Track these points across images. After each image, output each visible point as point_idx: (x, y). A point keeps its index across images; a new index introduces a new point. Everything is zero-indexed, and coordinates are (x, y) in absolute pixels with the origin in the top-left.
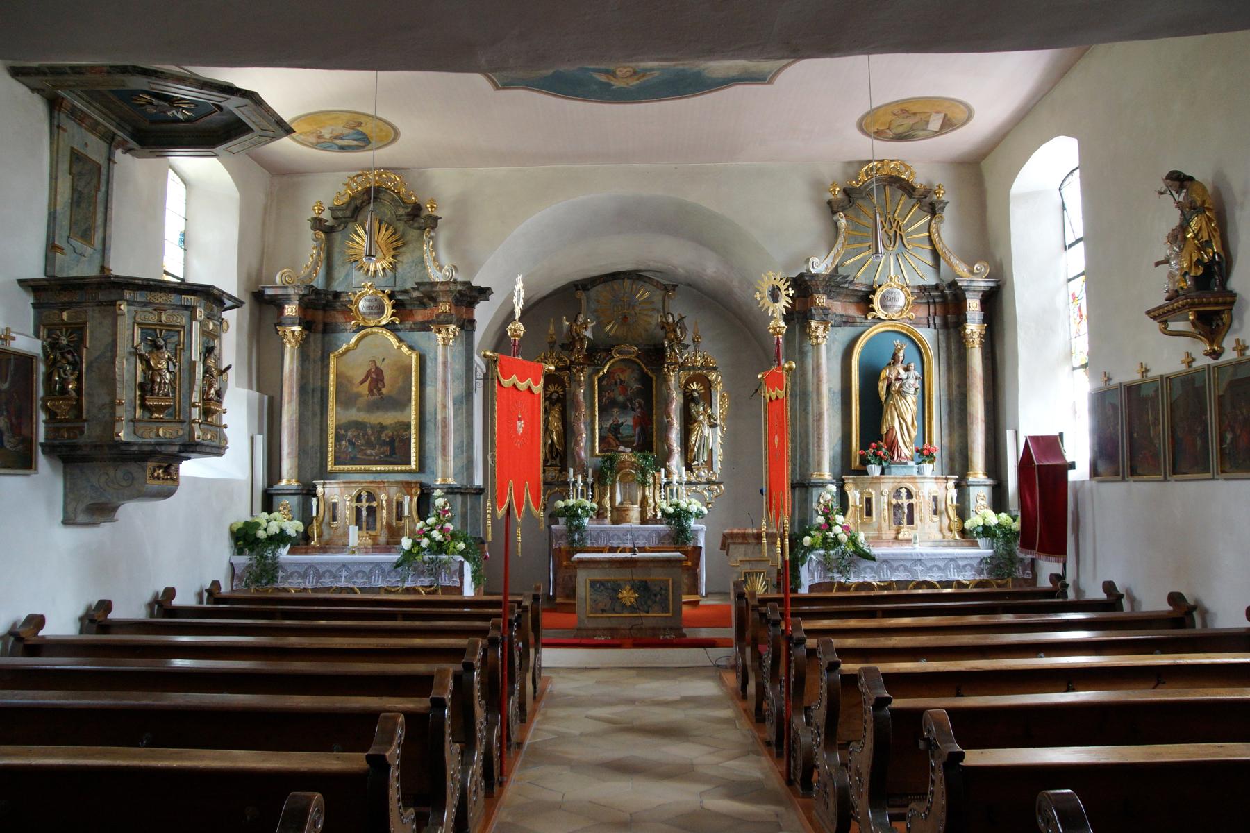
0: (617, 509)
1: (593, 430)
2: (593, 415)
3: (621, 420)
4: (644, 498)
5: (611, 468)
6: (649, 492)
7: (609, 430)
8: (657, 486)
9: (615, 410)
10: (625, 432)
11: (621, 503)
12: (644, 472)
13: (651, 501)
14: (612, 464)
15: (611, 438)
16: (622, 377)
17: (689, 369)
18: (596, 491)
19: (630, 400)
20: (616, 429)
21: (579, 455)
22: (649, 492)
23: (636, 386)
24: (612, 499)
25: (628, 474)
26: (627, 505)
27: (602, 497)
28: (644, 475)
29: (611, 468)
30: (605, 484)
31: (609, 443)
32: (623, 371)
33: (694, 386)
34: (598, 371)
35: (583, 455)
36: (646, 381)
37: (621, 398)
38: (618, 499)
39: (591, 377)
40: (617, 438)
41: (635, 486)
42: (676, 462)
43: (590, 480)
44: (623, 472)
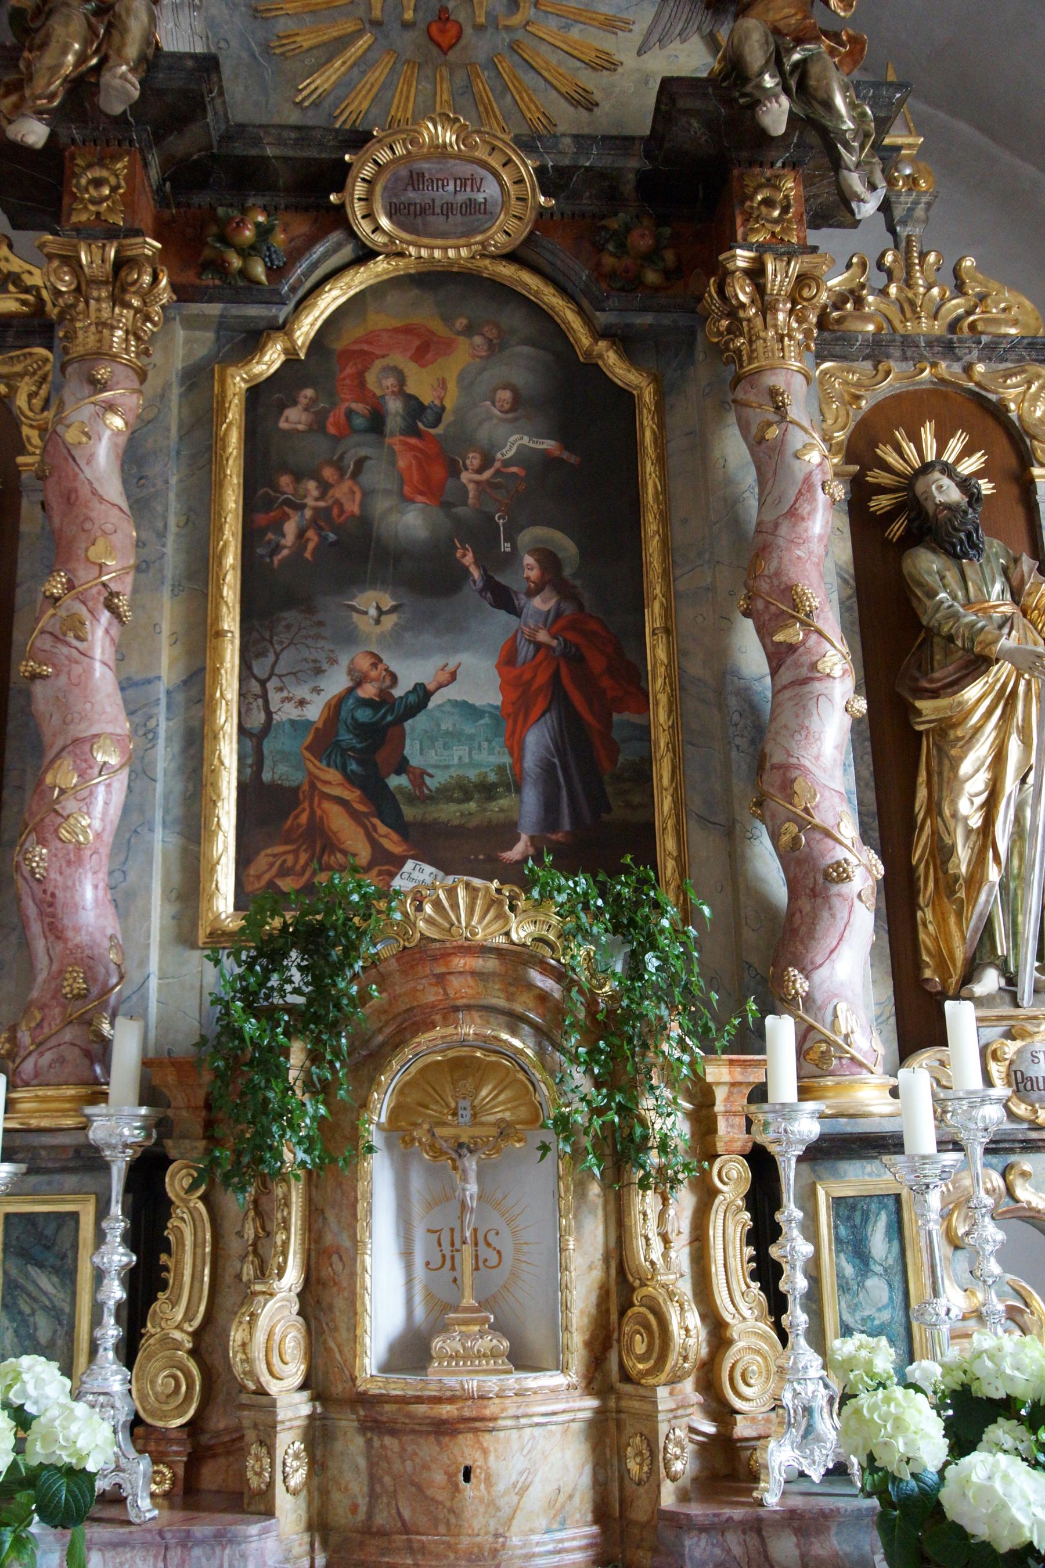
0: (375, 1414)
1: (196, 743)
2: (200, 637)
3: (411, 673)
4: (623, 1286)
5: (318, 1017)
6: (662, 1230)
7: (324, 741)
8: (733, 1177)
9: (371, 600)
10: (444, 753)
11: (412, 1351)
12: (615, 1044)
13: (687, 1328)
14: (321, 974)
15: (336, 795)
16: (422, 385)
17: (877, 351)
18: (188, 1227)
19: (483, 536)
20: (371, 736)
21: (53, 914)
22: (662, 1230)
23: (517, 442)
24: (327, 1303)
25: (462, 1068)
26: (465, 1371)
27: (229, 1296)
28: (620, 1077)
29: (318, 1017)
30: (255, 1165)
31: (320, 842)
32: (426, 348)
33: (903, 454)
34: (250, 341)
35: (88, 902)
36: (592, 426)
37: (412, 522)
38: (385, 1300)
39: (200, 379)
40: (381, 803)
41: (533, 1180)
42: (848, 971)
43: (119, 1125)
44: (429, 1045)
